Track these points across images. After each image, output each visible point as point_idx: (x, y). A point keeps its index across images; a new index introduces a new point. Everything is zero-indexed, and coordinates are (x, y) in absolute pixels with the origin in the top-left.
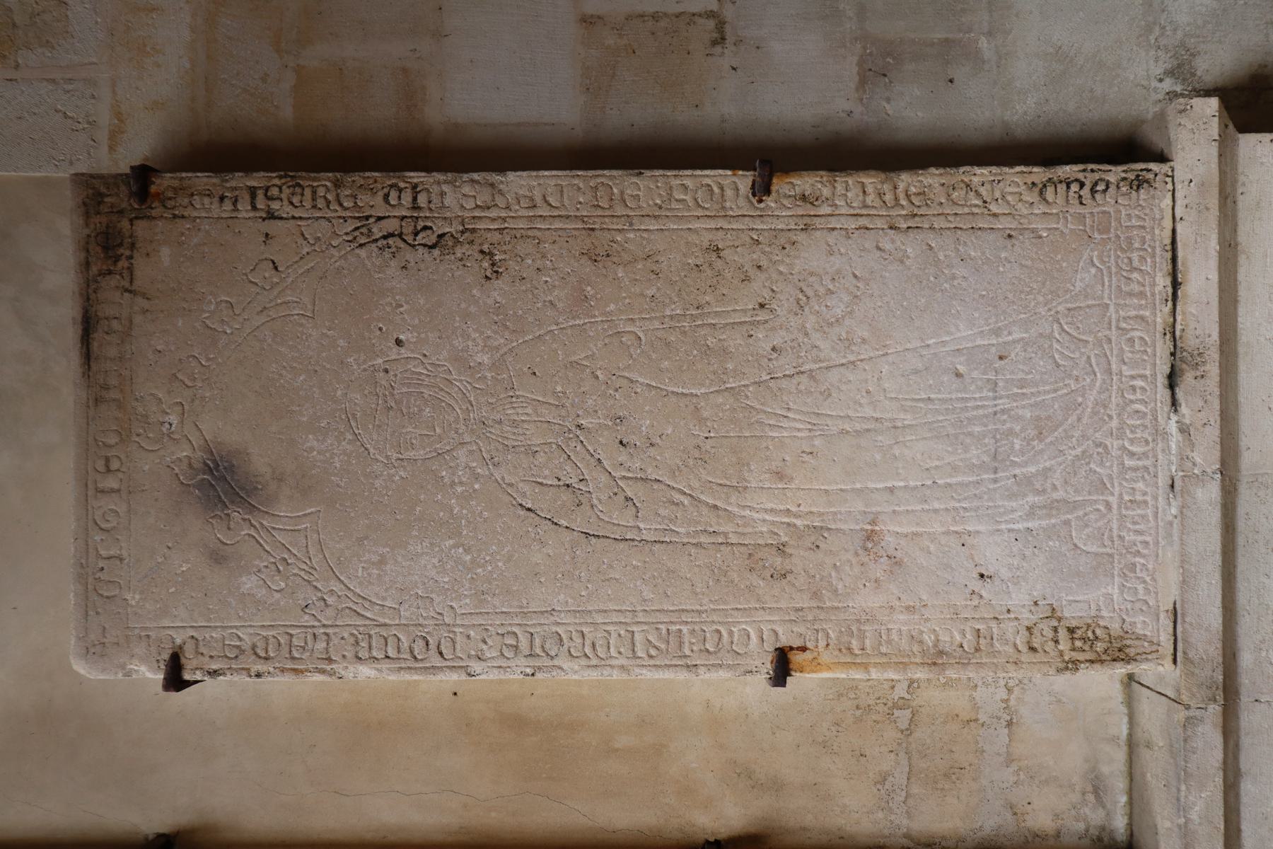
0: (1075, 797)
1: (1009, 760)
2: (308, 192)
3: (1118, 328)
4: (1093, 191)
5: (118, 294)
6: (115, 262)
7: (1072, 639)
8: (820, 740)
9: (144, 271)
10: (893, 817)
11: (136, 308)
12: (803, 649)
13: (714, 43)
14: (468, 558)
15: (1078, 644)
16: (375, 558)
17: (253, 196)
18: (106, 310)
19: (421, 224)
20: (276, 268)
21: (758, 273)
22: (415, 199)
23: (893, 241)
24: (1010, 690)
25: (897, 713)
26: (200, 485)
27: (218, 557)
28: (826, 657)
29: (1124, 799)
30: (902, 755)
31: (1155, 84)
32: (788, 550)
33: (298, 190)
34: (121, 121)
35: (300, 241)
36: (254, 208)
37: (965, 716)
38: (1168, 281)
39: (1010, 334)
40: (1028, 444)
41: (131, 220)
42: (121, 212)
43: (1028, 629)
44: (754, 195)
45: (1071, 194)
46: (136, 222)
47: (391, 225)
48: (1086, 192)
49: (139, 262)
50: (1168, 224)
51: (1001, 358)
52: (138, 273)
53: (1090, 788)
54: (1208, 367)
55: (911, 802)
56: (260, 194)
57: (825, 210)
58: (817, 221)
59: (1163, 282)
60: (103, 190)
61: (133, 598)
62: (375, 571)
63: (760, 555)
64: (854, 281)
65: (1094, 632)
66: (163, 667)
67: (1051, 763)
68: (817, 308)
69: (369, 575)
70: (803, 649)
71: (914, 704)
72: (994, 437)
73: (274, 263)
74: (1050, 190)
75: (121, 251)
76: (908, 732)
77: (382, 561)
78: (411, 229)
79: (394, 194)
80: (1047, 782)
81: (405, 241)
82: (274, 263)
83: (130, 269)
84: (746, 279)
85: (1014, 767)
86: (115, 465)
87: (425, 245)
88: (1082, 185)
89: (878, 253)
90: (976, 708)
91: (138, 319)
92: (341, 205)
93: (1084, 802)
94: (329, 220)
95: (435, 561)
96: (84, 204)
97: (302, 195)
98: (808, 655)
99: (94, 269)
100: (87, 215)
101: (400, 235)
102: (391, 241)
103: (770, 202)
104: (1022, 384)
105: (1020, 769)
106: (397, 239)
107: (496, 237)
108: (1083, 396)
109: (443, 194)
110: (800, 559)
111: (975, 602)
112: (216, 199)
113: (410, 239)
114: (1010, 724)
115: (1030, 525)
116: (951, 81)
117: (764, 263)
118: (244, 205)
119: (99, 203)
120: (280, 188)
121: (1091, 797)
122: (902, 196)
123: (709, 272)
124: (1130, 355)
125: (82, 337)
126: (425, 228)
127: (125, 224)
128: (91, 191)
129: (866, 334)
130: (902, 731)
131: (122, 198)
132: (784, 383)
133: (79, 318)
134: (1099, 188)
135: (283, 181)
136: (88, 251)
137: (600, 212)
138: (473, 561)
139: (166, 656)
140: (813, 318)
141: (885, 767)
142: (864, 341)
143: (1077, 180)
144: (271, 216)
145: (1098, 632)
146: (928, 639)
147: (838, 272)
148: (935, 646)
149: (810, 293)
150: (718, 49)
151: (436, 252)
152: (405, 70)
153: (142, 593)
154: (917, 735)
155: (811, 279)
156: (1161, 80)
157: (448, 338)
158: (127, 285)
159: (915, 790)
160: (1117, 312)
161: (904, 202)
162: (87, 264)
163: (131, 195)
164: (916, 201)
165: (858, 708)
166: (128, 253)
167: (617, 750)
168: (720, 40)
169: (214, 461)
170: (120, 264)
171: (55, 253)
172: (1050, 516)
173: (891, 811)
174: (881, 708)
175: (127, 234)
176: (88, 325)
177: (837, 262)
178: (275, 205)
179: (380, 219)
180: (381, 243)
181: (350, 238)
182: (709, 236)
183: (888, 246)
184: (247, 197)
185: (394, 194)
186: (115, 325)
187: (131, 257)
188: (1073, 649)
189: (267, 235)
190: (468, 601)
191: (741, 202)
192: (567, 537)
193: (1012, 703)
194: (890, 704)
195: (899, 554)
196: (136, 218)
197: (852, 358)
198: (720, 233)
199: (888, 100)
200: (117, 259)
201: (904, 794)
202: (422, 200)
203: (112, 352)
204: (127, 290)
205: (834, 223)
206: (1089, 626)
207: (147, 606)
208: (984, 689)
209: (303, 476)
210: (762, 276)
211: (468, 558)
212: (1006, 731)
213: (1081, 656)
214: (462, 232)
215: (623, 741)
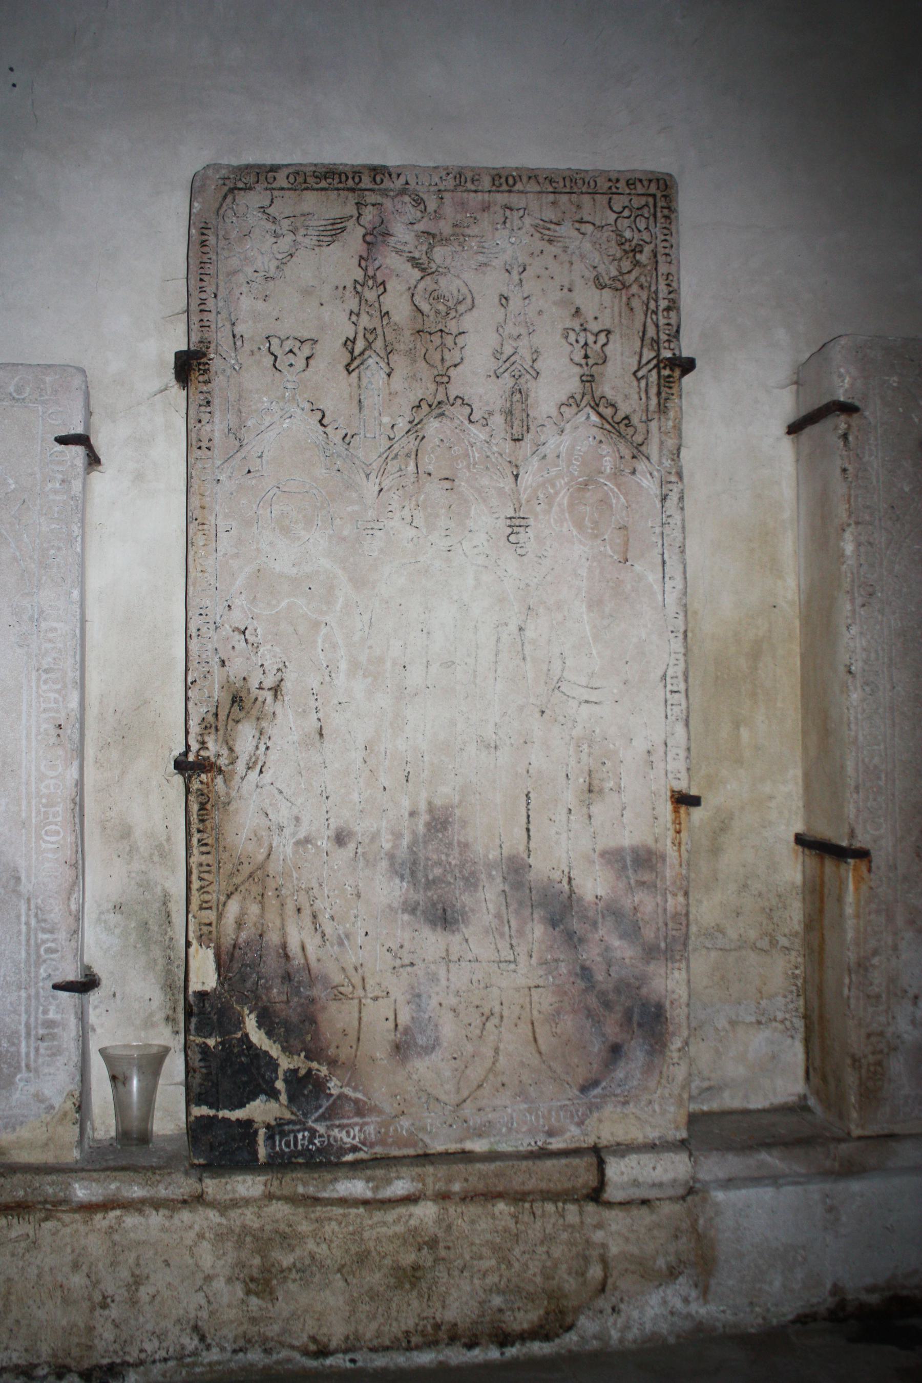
1: (733, 1023)
8: (749, 882)
12: (869, 870)
15: (872, 1068)
24: (782, 1022)
25: (767, 939)
28: (864, 888)
29: (705, 1108)
53: (712, 1083)
55: (704, 952)
66: (850, 401)
70: (869, 870)
71: (774, 951)
76: (754, 947)
80: (717, 1051)
85: (728, 1027)
90: (771, 997)
93: (703, 1079)
111: (899, 993)
121: (706, 1084)
130: (754, 944)
139: (857, 403)
146: (875, 961)
165: (771, 910)
174: (771, 926)
193: (774, 1024)
201: (710, 946)
213: (863, 1071)
215: (745, 733)
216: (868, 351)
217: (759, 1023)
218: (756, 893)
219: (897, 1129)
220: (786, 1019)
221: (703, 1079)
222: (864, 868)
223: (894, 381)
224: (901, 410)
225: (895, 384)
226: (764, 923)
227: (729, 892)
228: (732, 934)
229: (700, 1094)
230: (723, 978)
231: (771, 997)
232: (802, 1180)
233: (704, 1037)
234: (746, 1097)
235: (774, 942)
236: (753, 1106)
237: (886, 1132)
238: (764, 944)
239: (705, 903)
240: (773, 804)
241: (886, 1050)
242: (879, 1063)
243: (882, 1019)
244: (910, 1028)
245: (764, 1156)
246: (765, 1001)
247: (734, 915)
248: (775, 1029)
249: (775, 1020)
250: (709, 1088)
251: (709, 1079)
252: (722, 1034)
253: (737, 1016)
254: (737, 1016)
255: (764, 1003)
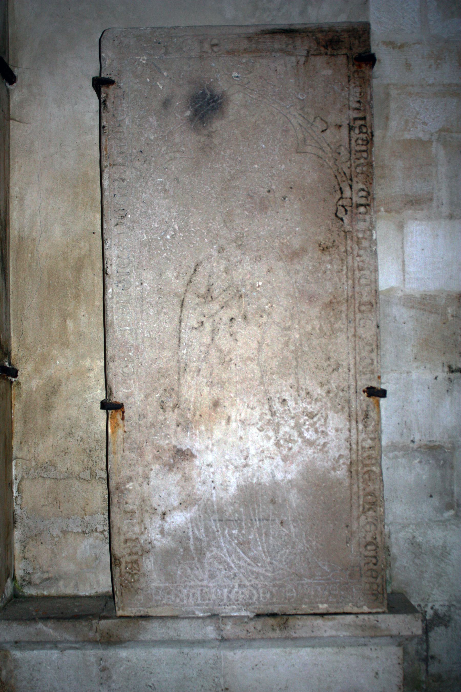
0: (45, 568)
1: (64, 532)
2: (364, 148)
3: (298, 584)
4: (372, 570)
5: (307, 48)
6: (324, 46)
7: (132, 562)
8: (73, 431)
9: (319, 62)
10: (32, 470)
11: (299, 57)
12: (123, 419)
13: (450, 367)
14: (168, 237)
15: (130, 566)
16: (167, 187)
17: (361, 119)
18: (298, 43)
19: (349, 209)
20: (323, 131)
21: (326, 391)
22: (362, 205)
23: (344, 464)
25: (88, 472)
26: (204, 94)
27: (166, 103)
29: (46, 593)
30: (66, 475)
31: (430, 605)
32: (176, 410)
33: (365, 143)
34: (399, 48)
35: (338, 144)
36: (355, 119)
37: (87, 508)
38: (325, 611)
39: (294, 527)
40: (235, 538)
41: (346, 54)
42: (351, 49)
43: (137, 539)
44: (368, 388)
45: (370, 559)
46: (345, 57)
47: (347, 193)
48: (371, 566)
49: (324, 59)
50: (355, 610)
51: (282, 523)
52: (318, 58)
53: (50, 575)
54: (278, 632)
55: (41, 480)
56: (362, 122)
57: (361, 427)
58: (354, 423)
59: (323, 607)
60: (362, 39)
61: (144, 60)
62: (160, 188)
63: (173, 395)
64: (322, 443)
65: (136, 574)
67: (63, 555)
68: (307, 423)
69: (158, 185)
70: (123, 419)
71: (93, 481)
72: (239, 519)
73: (325, 130)
74: (373, 547)
75: (330, 49)
76: (78, 478)
77: (165, 191)
78: (345, 203)
79: (364, 194)
80: (53, 552)
81: (339, 200)
82: (325, 130)
83: (320, 54)
84: (322, 385)
86: (216, 49)
87: (337, 211)
88: (375, 564)
89: (337, 455)
90: (92, 514)
91: (293, 59)
92: (358, 165)
93: (43, 572)
94: (350, 159)
95: (167, 220)
96: (354, 29)
97: (362, 145)
98: (120, 421)
99: (319, 35)
100: (348, 31)
101: (341, 198)
102: (339, 192)
103: (364, 396)
104: (267, 535)
105: (60, 538)
106: (340, 196)
107: (343, 249)
108: (262, 566)
109: (365, 221)
110: (172, 417)
112: (358, 100)
113: (340, 203)
114: (84, 532)
115: (192, 539)
116: (431, 496)
117: (331, 395)
118: (355, 115)
119: (355, 37)
120: (366, 133)
121: (46, 576)
122: (369, 468)
123: (326, 364)
124: (284, 591)
125: (283, 29)
126: (346, 211)
127: (344, 51)
128: (361, 32)
129: (293, 450)
131: (358, 50)
132: (267, 406)
133: (292, 27)
134: (374, 573)
135: (370, 134)
136: (329, 32)
137: (357, 305)
138: (167, 240)
139: (113, 78)
140: (302, 421)
141: (59, 466)
142: (290, 449)
143: (377, 561)
144: (351, 128)
145: (136, 577)
146: (129, 486)
147: (327, 434)
148: (126, 489)
149: (315, 419)
150: (446, 369)
151: (333, 217)
152: (431, 200)
153: (147, 64)
154: (77, 483)
155: (323, 420)
156: (432, 608)
157: (287, 224)
158: (312, 52)
159: (48, 482)
160: (307, 584)
161: (365, 469)
162: (321, 31)
163: (360, 54)
164: (366, 476)
165: (90, 451)
166: (329, 53)
167: (65, 321)
168: (451, 370)
169: (218, 100)
170: (322, 49)
171: (327, 13)
172: (196, 549)
173: (37, 469)
175: (338, 52)
176: (290, 32)
177: (332, 433)
178: (357, 131)
179: (351, 187)
180: (337, 187)
181: (340, 171)
182: (345, 364)
183: (341, 461)
184: (360, 115)
185: (364, 194)
186: (290, 47)
187: (326, 54)
188: (126, 562)
189: (340, 126)
190: (145, 238)
191: (364, 382)
192: (181, 290)
193: (95, 534)
194: (93, 468)
195: (175, 469)
196: (348, 57)
197: (282, 442)
198: (346, 370)
199: (420, 462)
200: (326, 47)
201: (45, 476)
202: (362, 209)
203: (277, 46)
204: (308, 52)
205: (354, 431)
206: (139, 571)
207: (139, 67)
208: (102, 519)
209: (211, 148)
210: (324, 394)
211: (168, 237)
212: (80, 531)
214: (344, 231)
215: (70, 324)
216: (123, 39)
217: (84, 532)
218: (79, 438)
219: (152, 612)
220: (104, 530)
221: (43, 572)
222: (119, 417)
223: (144, 60)
224: (148, 80)
225: (144, 62)
226: (85, 460)
227: (58, 438)
228: (61, 467)
229: (41, 583)
230: (55, 499)
231: (92, 514)
232: (77, 646)
233: (42, 541)
234: (76, 586)
235: (94, 474)
236: (82, 593)
237: (142, 613)
238: (87, 475)
239: (41, 445)
240: (91, 375)
241: (140, 553)
242: (136, 562)
243: (137, 529)
244: (159, 536)
245: (40, 626)
246: (87, 516)
247: (63, 454)
248: (97, 538)
249: (96, 531)
250: (48, 579)
251: (48, 572)
252: (56, 539)
253: (67, 527)
254: (67, 527)
255: (87, 518)
